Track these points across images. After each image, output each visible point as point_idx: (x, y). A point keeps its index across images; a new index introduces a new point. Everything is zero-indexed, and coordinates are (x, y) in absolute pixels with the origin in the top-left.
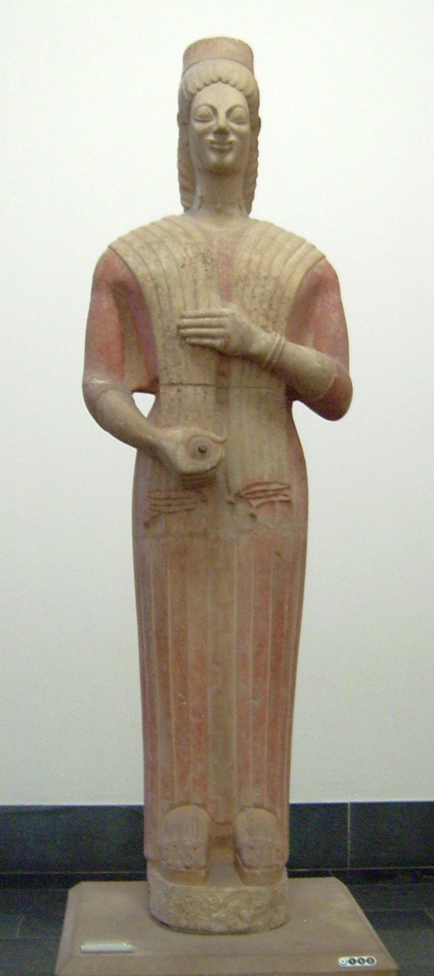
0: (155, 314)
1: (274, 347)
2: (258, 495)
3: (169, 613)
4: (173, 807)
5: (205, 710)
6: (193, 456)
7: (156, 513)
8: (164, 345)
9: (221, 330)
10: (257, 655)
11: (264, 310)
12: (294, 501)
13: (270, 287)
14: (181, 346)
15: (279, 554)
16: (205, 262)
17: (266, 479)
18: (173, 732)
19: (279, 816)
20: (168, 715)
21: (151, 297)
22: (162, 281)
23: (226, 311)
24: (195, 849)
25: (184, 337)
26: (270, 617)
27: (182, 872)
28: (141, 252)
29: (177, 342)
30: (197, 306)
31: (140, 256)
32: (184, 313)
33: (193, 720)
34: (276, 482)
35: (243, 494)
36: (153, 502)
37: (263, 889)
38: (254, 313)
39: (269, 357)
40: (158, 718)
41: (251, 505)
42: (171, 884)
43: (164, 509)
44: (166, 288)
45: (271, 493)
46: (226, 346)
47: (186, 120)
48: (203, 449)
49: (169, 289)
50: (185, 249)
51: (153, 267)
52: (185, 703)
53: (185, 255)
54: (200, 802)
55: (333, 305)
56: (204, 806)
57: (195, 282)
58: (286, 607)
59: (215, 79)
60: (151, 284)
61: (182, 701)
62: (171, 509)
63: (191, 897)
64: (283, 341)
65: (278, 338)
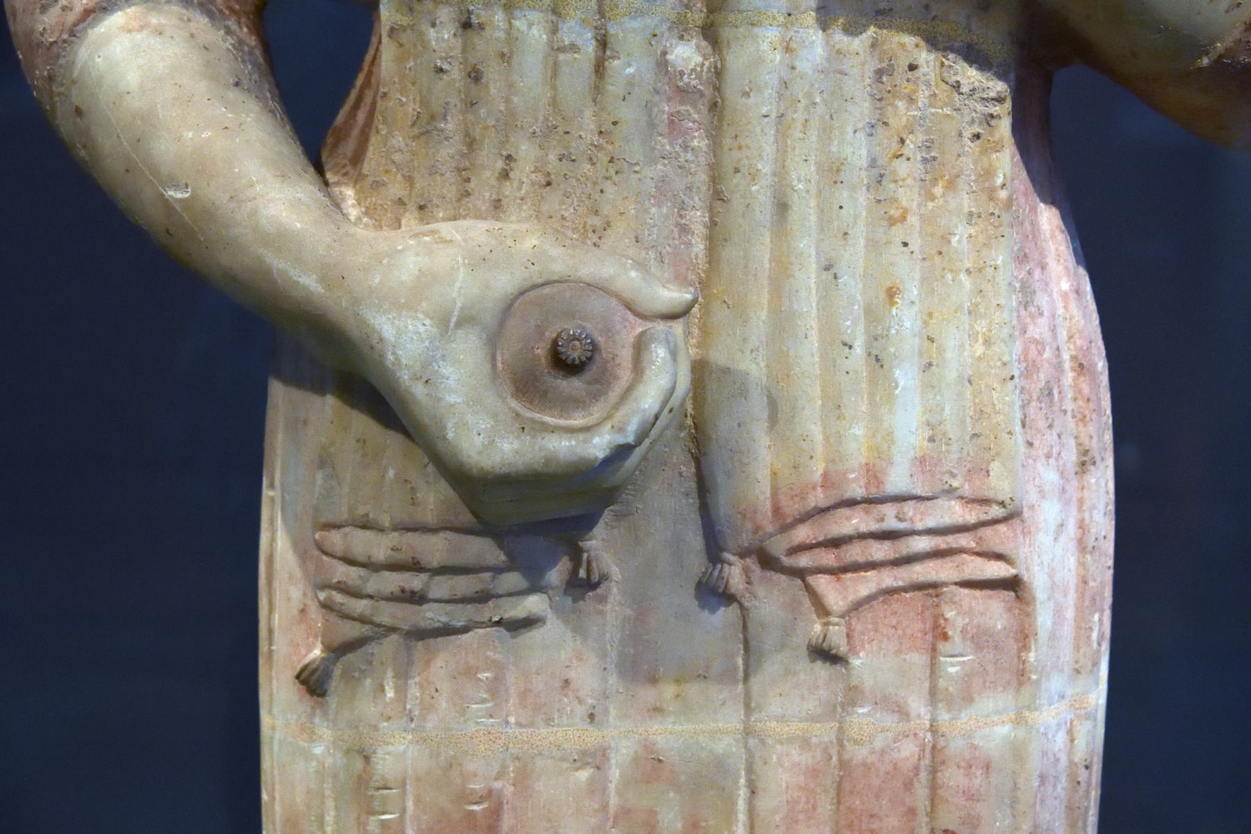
2: (855, 553)
7: (352, 630)
12: (1038, 581)
17: (898, 479)
34: (950, 492)
35: (778, 546)
36: (342, 572)
41: (822, 609)
43: (388, 614)
45: (922, 544)
48: (575, 353)
62: (432, 615)
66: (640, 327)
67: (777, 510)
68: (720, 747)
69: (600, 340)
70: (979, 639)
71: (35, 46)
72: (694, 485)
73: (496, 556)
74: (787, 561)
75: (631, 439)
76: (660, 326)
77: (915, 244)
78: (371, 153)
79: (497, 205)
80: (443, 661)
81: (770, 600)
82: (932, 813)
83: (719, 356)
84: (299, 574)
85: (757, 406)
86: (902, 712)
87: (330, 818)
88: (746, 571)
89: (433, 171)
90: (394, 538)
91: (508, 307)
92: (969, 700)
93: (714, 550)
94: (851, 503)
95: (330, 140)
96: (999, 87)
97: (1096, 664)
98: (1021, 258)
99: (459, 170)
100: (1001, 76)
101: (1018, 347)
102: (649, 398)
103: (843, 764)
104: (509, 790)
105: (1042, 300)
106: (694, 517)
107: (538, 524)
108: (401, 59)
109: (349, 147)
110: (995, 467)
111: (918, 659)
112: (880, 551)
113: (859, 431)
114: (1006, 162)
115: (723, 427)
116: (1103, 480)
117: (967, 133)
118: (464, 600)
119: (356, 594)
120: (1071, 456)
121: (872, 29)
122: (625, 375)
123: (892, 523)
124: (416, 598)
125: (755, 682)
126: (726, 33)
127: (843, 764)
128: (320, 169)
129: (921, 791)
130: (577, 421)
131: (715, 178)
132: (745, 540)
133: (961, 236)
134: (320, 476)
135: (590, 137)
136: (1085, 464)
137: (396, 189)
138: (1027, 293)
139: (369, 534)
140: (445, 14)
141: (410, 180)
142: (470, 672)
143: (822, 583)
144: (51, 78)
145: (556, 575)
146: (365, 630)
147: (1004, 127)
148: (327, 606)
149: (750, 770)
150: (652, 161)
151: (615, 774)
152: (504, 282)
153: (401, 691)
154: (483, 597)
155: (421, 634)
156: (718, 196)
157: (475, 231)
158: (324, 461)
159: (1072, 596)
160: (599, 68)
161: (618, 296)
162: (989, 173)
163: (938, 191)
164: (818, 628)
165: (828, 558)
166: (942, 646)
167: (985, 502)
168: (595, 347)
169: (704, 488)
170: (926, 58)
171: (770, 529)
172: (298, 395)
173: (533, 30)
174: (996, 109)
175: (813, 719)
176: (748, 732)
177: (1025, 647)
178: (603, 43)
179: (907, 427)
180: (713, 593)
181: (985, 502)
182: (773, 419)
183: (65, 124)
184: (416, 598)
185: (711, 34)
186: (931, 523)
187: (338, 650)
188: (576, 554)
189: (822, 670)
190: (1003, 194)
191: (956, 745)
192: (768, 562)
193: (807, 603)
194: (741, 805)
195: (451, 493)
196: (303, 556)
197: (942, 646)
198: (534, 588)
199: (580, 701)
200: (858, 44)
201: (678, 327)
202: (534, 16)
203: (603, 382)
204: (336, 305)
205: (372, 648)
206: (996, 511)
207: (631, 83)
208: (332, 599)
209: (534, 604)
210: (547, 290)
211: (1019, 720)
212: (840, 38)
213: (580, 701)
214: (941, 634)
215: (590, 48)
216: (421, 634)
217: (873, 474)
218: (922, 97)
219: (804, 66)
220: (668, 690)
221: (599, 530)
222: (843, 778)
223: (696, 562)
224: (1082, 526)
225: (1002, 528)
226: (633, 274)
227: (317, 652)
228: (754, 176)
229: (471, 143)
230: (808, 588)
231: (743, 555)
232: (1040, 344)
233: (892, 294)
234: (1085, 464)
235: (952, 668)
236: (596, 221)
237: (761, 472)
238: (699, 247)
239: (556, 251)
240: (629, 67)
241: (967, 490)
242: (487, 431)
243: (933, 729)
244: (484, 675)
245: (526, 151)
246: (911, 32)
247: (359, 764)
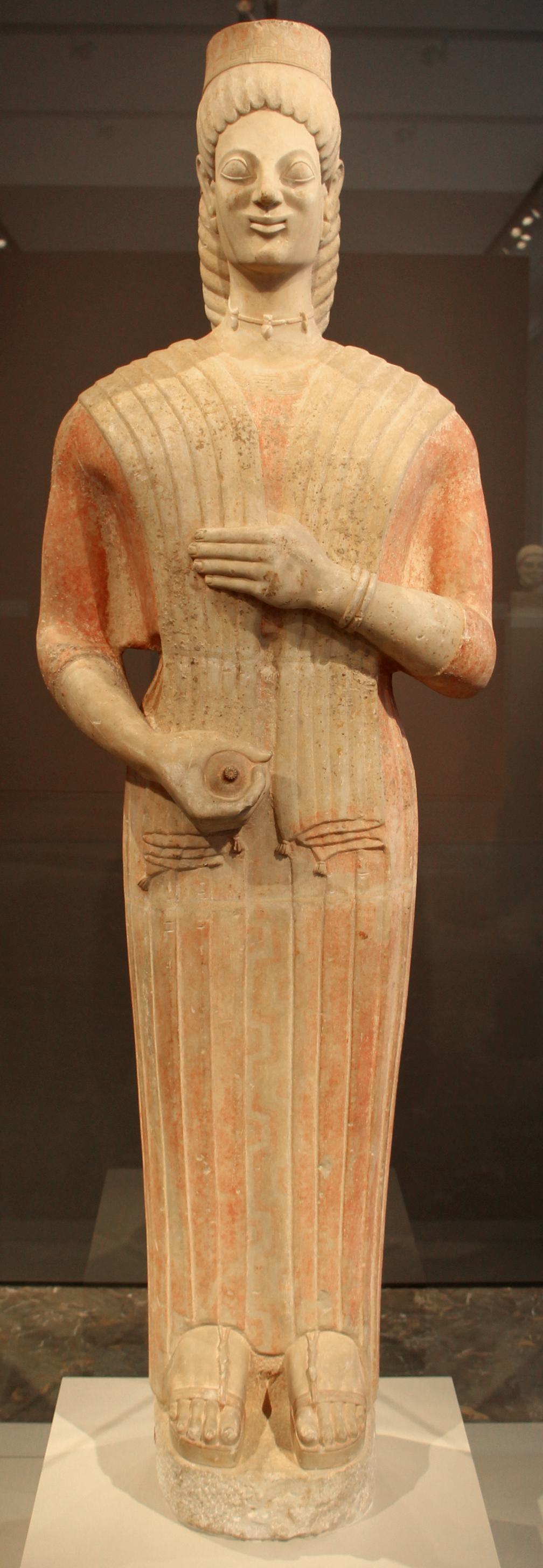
0: (152, 530)
1: (357, 597)
2: (328, 839)
3: (181, 1030)
4: (190, 1327)
5: (241, 1183)
6: (215, 787)
7: (157, 869)
8: (168, 585)
9: (264, 568)
10: (325, 1096)
11: (341, 521)
12: (391, 847)
13: (353, 478)
14: (196, 588)
15: (364, 936)
16: (238, 437)
17: (343, 814)
18: (189, 1214)
19: (361, 1340)
20: (180, 1186)
21: (144, 500)
22: (161, 471)
23: (273, 531)
24: (222, 1406)
25: (203, 575)
26: (349, 1037)
27: (200, 1447)
28: (130, 417)
29: (190, 579)
30: (223, 520)
31: (127, 424)
32: (201, 532)
33: (221, 1197)
34: (360, 818)
35: (302, 838)
36: (152, 849)
37: (331, 1473)
38: (323, 529)
39: (345, 615)
40: (165, 1189)
41: (318, 859)
42: (184, 1462)
43: (169, 863)
44: (170, 486)
45: (351, 836)
46: (271, 594)
47: (210, 172)
48: (231, 776)
49: (175, 489)
50: (205, 415)
51: (148, 447)
52: (207, 1172)
53: (204, 426)
54: (233, 1322)
55: (466, 498)
56: (239, 1328)
57: (221, 476)
58: (376, 1018)
59: (257, 103)
60: (144, 478)
61: (202, 1168)
62: (183, 863)
63: (213, 1485)
64: (372, 586)
65: (364, 579)
66: (253, 766)
67: (301, 825)
68: (283, 907)
69: (240, 770)
70: (371, 867)
71: (48, 673)
72: (272, 817)
73: (207, 844)
74: (305, 843)
75: (250, 804)
76: (260, 765)
77: (347, 734)
78: (160, 706)
79: (204, 723)
80: (188, 879)
81: (300, 856)
82: (356, 926)
83: (280, 773)
84: (137, 849)
85: (294, 789)
86: (346, 893)
87: (151, 932)
88: (291, 846)
89: (181, 712)
90: (170, 837)
91: (208, 761)
92: (368, 887)
93: (280, 839)
94: (327, 822)
95: (145, 699)
96: (373, 681)
97: (412, 873)
98: (383, 737)
99: (190, 711)
100: (374, 677)
101: (382, 768)
102: (256, 790)
103: (326, 911)
104: (211, 922)
105: (390, 751)
106: (273, 828)
107: (220, 833)
108: (170, 674)
109: (152, 703)
110: (375, 809)
111: (351, 875)
112: (337, 838)
113: (329, 797)
114: (377, 705)
115: (282, 798)
116: (414, 809)
117: (363, 697)
118: (195, 858)
119: (157, 856)
120: (402, 804)
121: (329, 663)
122: (248, 782)
123: (341, 829)
124: (178, 858)
125: (295, 884)
126: (280, 664)
127: (326, 911)
128: (141, 709)
129: (352, 919)
130: (232, 799)
131: (278, 713)
132: (291, 836)
133: (362, 731)
134: (144, 818)
135: (236, 700)
136: (406, 806)
137: (168, 718)
138: (385, 748)
139: (161, 836)
140: (185, 659)
141: (173, 715)
142: (197, 883)
143: (318, 850)
144: (54, 684)
145: (226, 848)
146: (161, 869)
147: (375, 694)
148: (148, 861)
149: (294, 913)
150: (256, 707)
151: (247, 916)
152: (207, 752)
153: (174, 889)
154: (201, 857)
155: (180, 870)
156: (279, 719)
157: (195, 735)
158: (145, 811)
159: (403, 851)
160: (238, 677)
161: (244, 755)
162: (370, 710)
163: (354, 716)
164: (316, 865)
165: (319, 841)
166: (359, 870)
167: (372, 821)
168: (238, 773)
169: (276, 818)
170: (348, 672)
171: (299, 832)
172: (136, 788)
173: (214, 664)
174: (372, 688)
175: (316, 896)
176: (293, 901)
177: (387, 869)
178: (239, 669)
179: (345, 795)
180: (280, 855)
181: (372, 821)
182: (300, 794)
183: (58, 698)
184: (178, 858)
185: (275, 664)
186: (354, 829)
187: (152, 875)
188: (233, 842)
189: (318, 879)
190: (376, 716)
191: (364, 903)
192: (299, 843)
193: (312, 856)
194: (291, 925)
195: (190, 822)
196: (139, 843)
197: (359, 870)
198: (219, 854)
199: (235, 892)
200: (325, 667)
201: (266, 765)
202: (215, 660)
203: (241, 784)
204: (150, 761)
205: (164, 875)
206: (376, 824)
207: (248, 681)
208: (150, 858)
209: (218, 859)
210: (221, 754)
211: (385, 894)
212: (318, 665)
213: (235, 892)
214: (358, 866)
215: (235, 670)
216: (180, 870)
217: (334, 813)
218: (347, 684)
219: (307, 675)
220: (266, 887)
221: (241, 833)
222: (326, 916)
223: (275, 844)
224: (406, 827)
225: (378, 829)
226: (250, 747)
227: (144, 876)
228: (291, 712)
229: (195, 703)
230: (313, 851)
231: (290, 841)
232: (390, 766)
233: (339, 751)
234: (406, 806)
235: (362, 877)
236: (238, 728)
237: (297, 813)
238: (273, 736)
239: (224, 741)
240: (247, 676)
241: (366, 817)
242: (203, 802)
243: (356, 898)
244: (202, 884)
245: (213, 705)
246: (343, 663)
247: (160, 914)
